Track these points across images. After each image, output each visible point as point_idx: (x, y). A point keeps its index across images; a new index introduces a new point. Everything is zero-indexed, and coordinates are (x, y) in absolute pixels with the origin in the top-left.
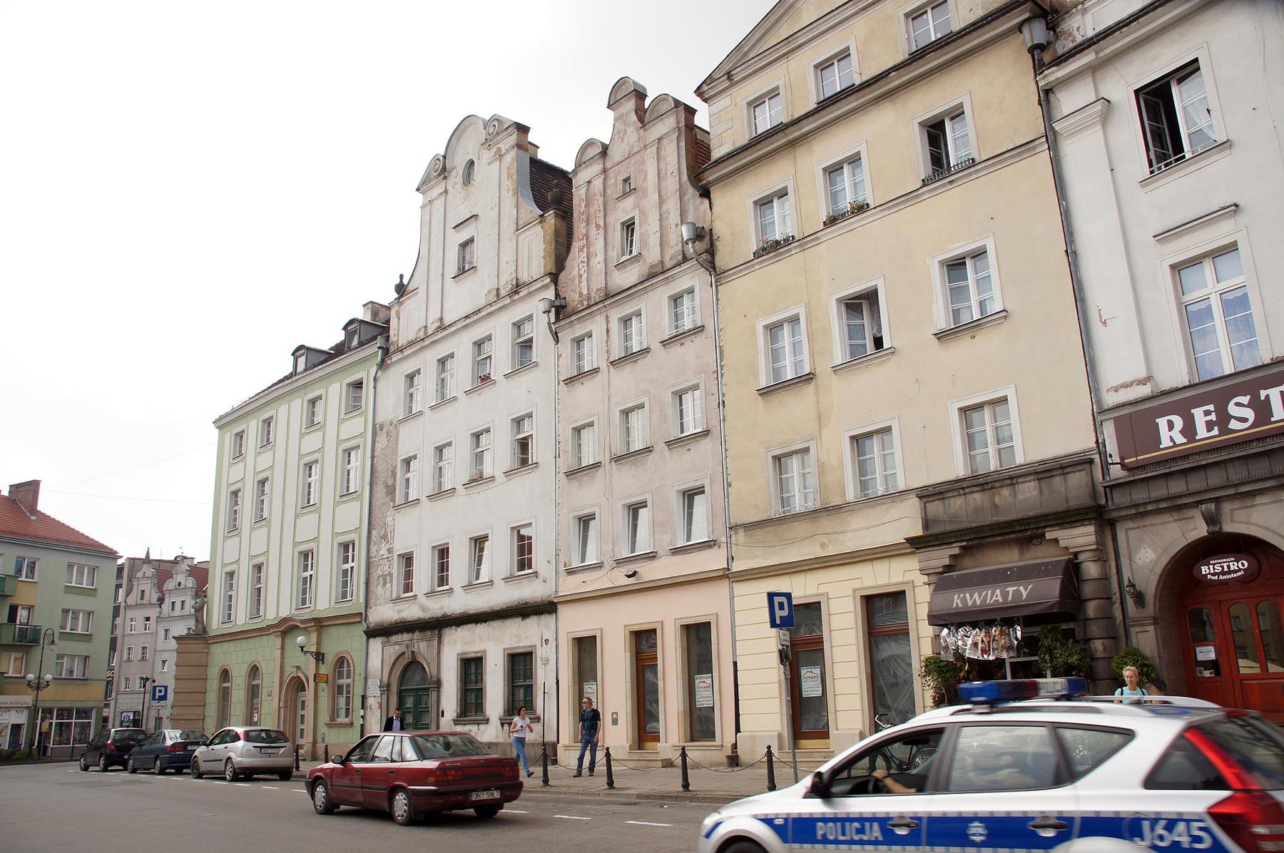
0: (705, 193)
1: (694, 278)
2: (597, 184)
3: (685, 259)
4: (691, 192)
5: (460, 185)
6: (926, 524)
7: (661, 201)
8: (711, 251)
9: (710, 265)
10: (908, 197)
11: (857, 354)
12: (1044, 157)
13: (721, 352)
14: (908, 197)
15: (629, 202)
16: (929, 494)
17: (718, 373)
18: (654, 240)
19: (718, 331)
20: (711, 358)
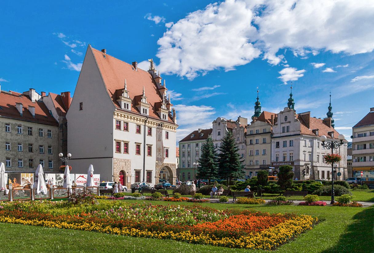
0: (246, 137)
1: (244, 144)
2: (235, 132)
3: (244, 143)
4: (244, 136)
5: (218, 125)
6: (260, 167)
7: (242, 136)
8: (246, 143)
9: (246, 144)
10: (262, 144)
11: (256, 154)
12: (270, 144)
13: (246, 152)
14: (262, 144)
15: (238, 135)
16: (260, 165)
17: (246, 153)
18: (241, 140)
19: (246, 150)
20: (245, 152)
